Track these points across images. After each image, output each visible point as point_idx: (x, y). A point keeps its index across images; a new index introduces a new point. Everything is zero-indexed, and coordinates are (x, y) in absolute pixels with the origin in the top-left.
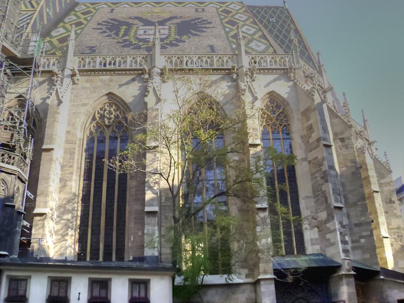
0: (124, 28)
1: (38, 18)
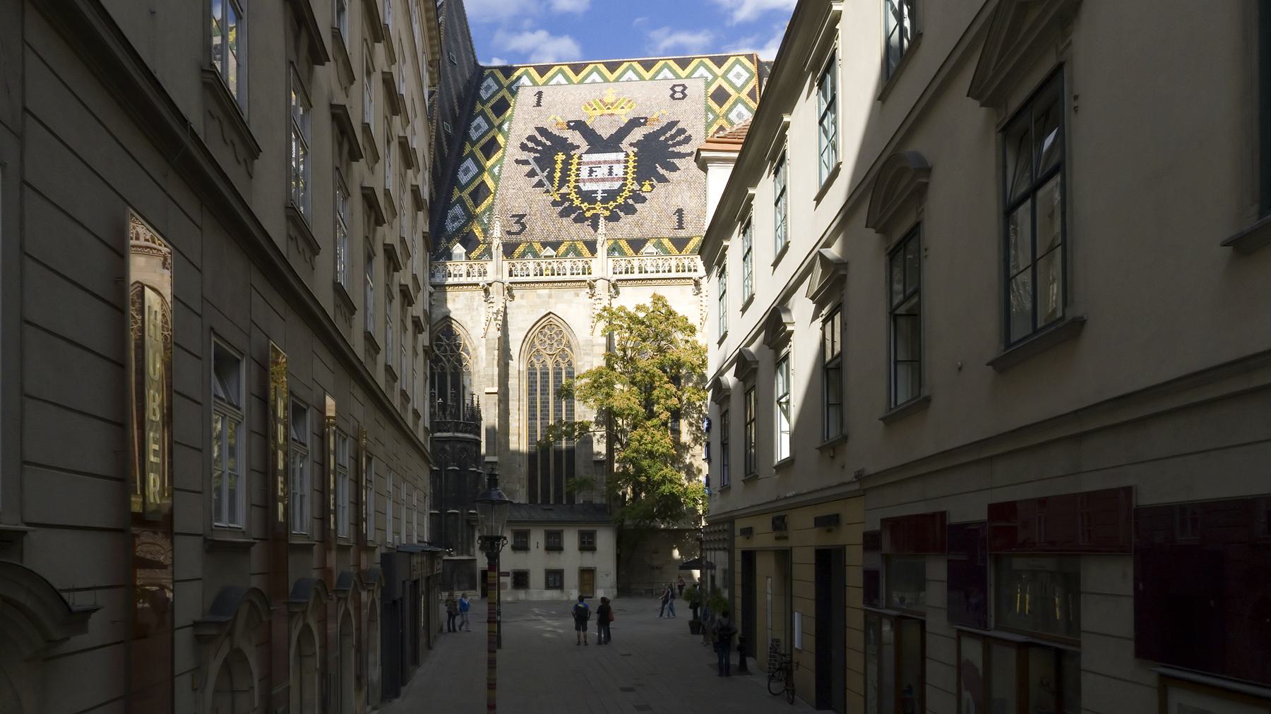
0: (560, 157)
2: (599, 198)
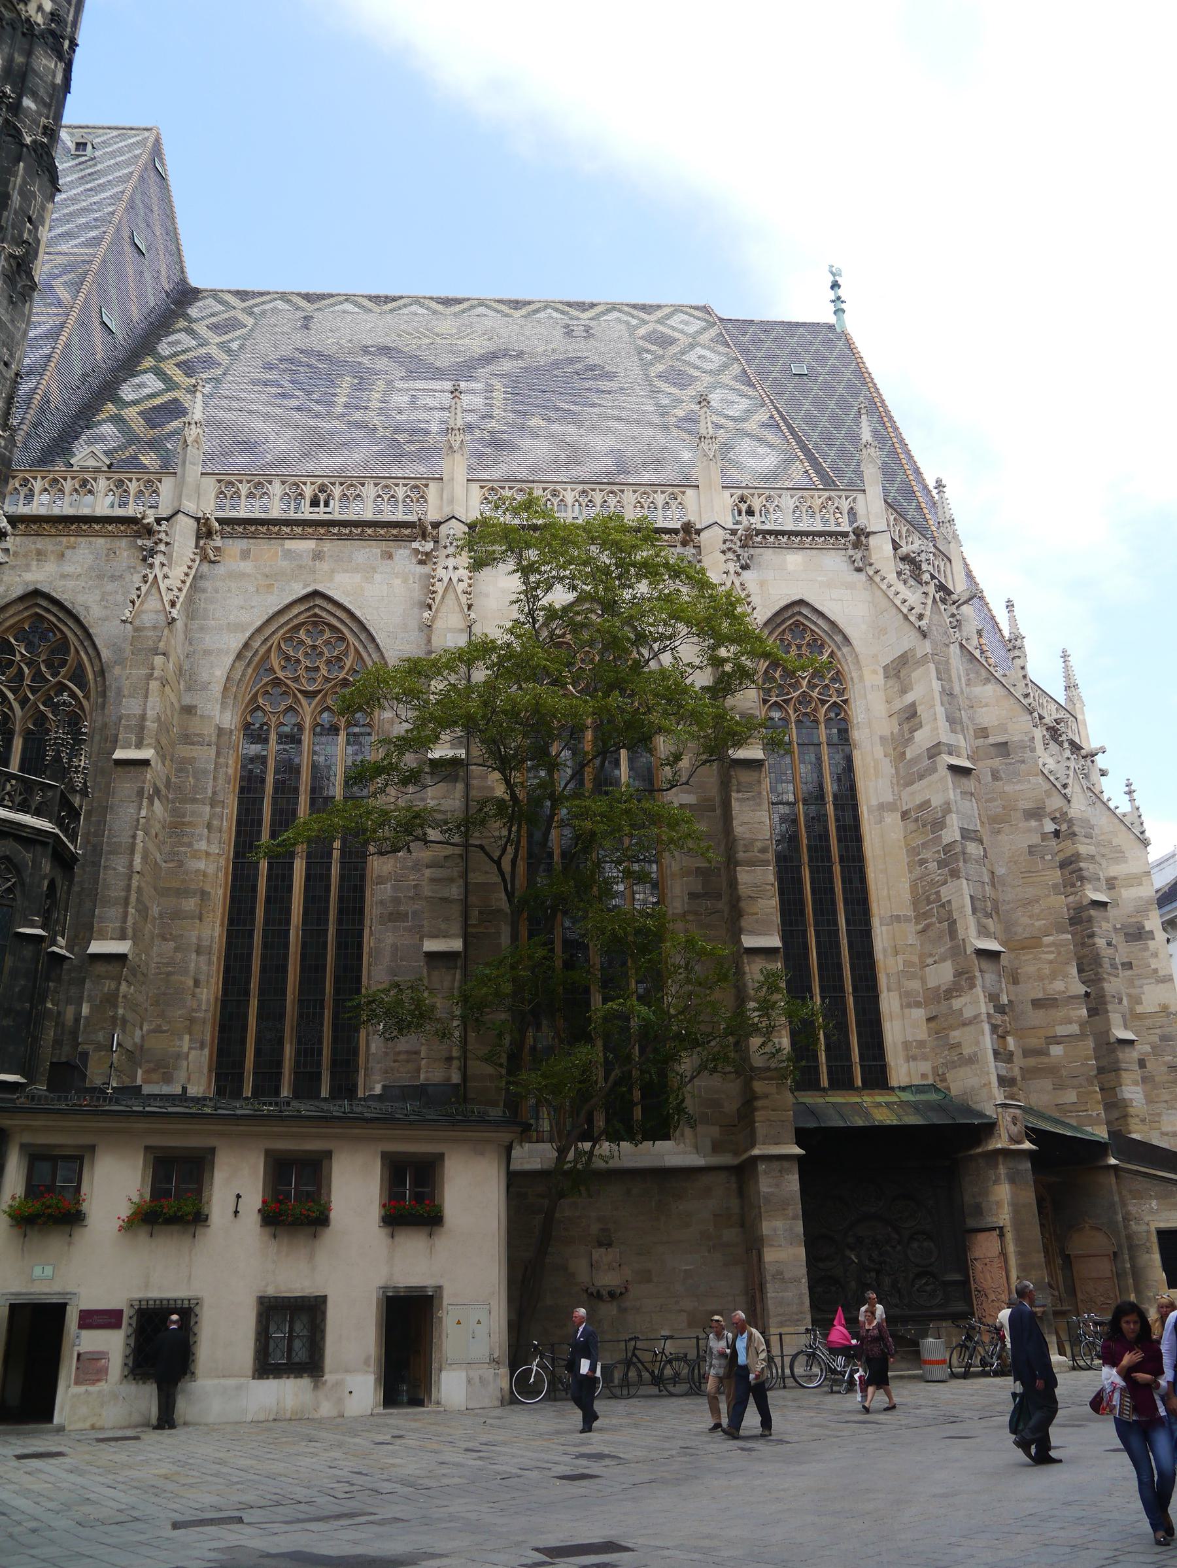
2: (434, 429)
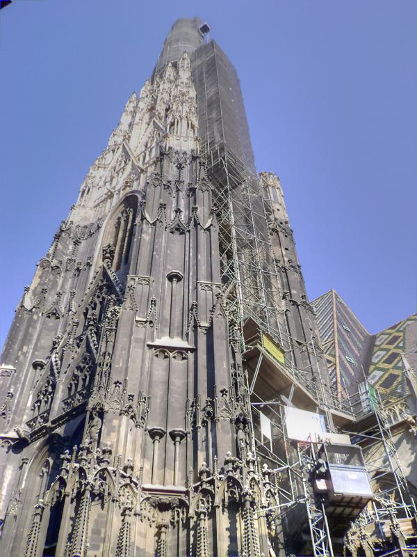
1: (342, 371)
